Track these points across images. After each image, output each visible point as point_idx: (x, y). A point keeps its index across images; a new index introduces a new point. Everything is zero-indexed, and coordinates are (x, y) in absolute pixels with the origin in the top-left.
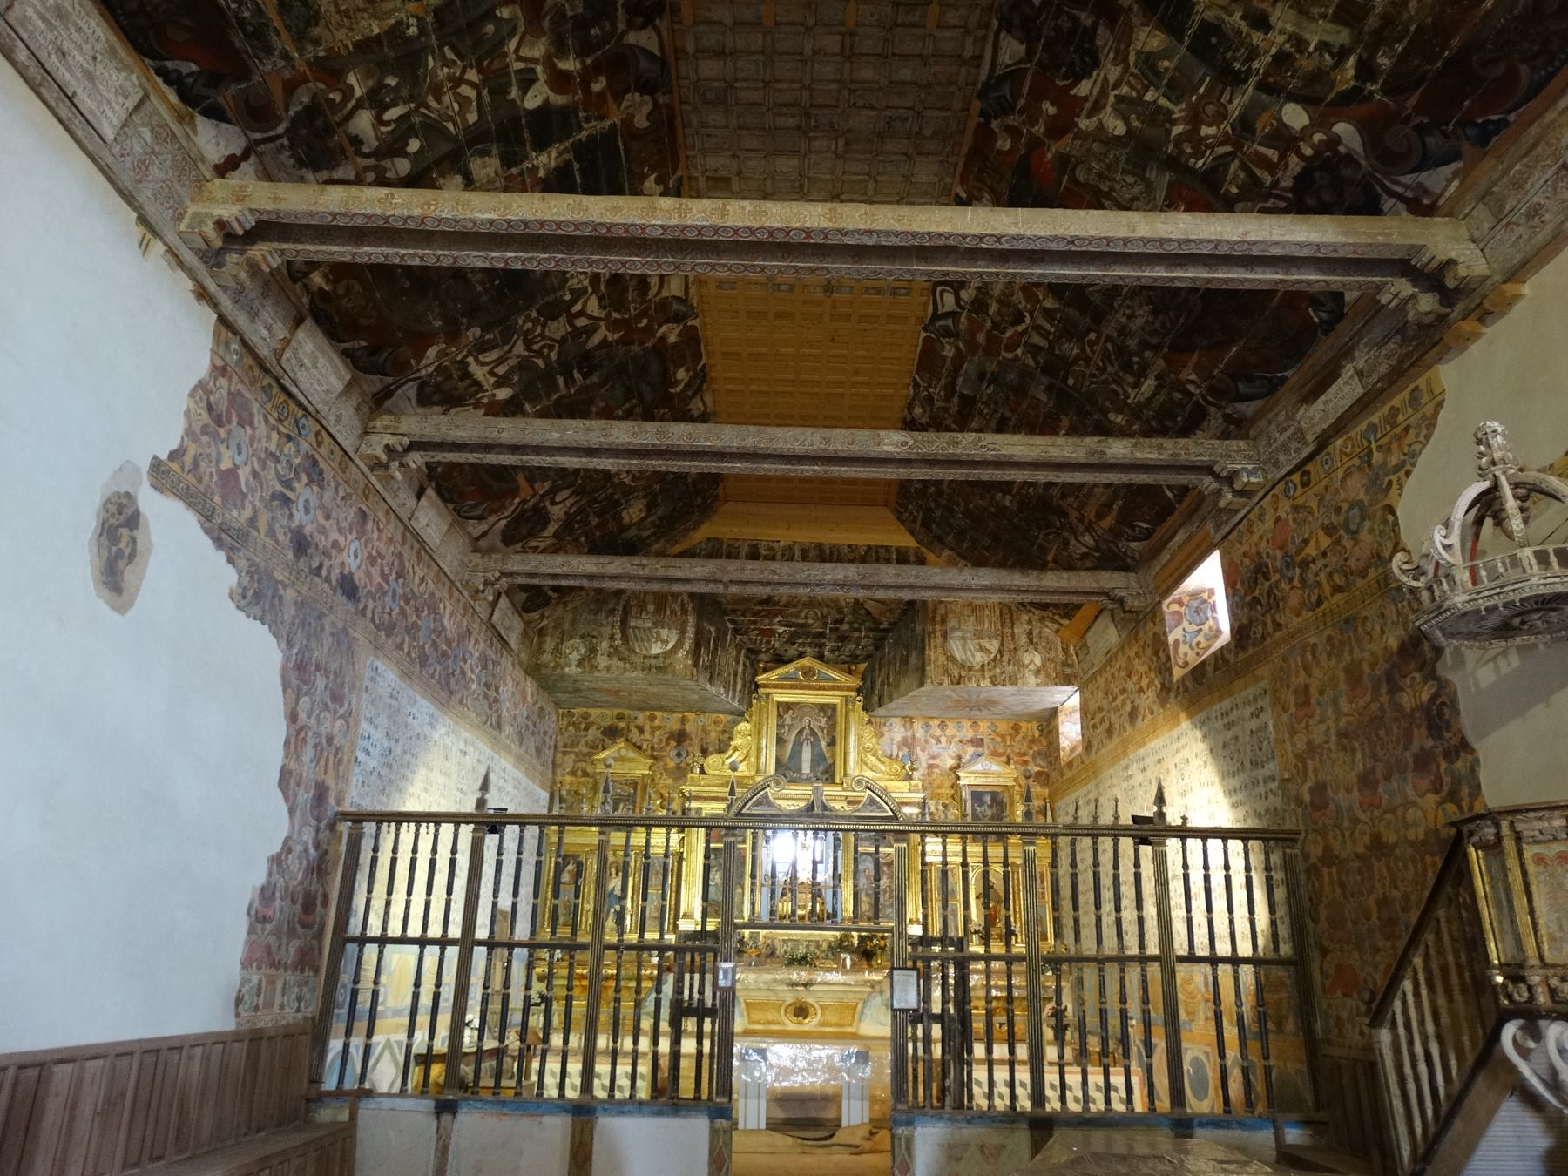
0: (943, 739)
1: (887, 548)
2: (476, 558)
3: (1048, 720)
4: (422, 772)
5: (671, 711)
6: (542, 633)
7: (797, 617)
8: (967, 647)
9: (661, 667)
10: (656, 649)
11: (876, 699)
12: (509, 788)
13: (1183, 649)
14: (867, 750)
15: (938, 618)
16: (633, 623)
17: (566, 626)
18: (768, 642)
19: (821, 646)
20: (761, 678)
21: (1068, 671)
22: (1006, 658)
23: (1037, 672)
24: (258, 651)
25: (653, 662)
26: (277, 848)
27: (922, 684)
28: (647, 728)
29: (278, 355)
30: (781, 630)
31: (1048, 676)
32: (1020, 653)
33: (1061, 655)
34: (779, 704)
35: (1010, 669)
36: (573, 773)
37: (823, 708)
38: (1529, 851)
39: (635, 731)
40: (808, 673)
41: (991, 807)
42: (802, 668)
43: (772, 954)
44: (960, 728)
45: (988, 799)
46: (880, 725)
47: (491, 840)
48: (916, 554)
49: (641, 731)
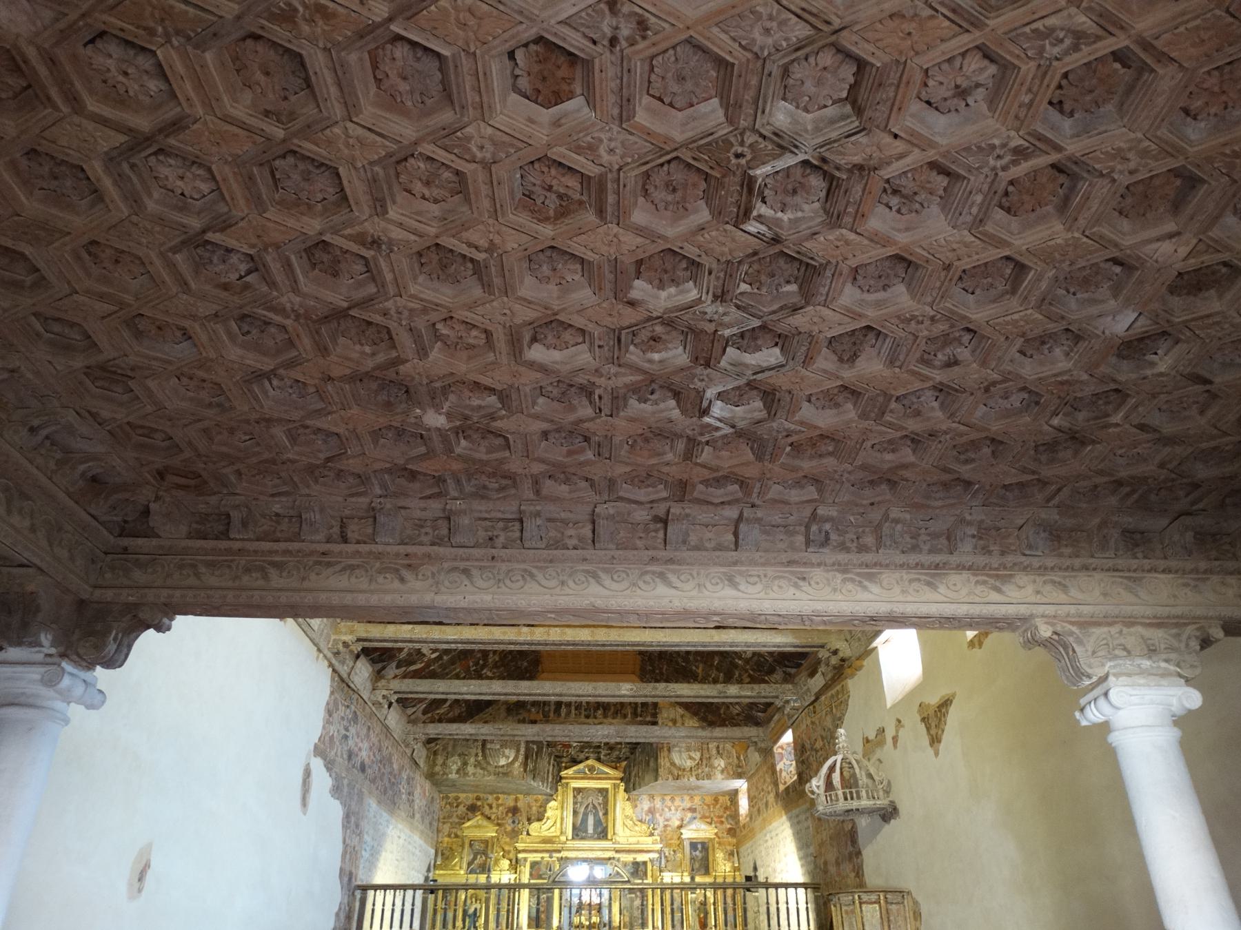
2: (410, 727)
3: (735, 793)
4: (383, 854)
5: (509, 794)
6: (435, 753)
8: (682, 758)
9: (505, 773)
10: (503, 762)
12: (417, 852)
13: (784, 774)
14: (627, 817)
17: (450, 749)
20: (563, 773)
23: (722, 772)
24: (336, 810)
26: (336, 909)
29: (349, 674)
34: (575, 789)
36: (449, 836)
38: (844, 908)
40: (592, 769)
44: (683, 800)
46: (635, 800)
47: (431, 897)
49: (491, 807)
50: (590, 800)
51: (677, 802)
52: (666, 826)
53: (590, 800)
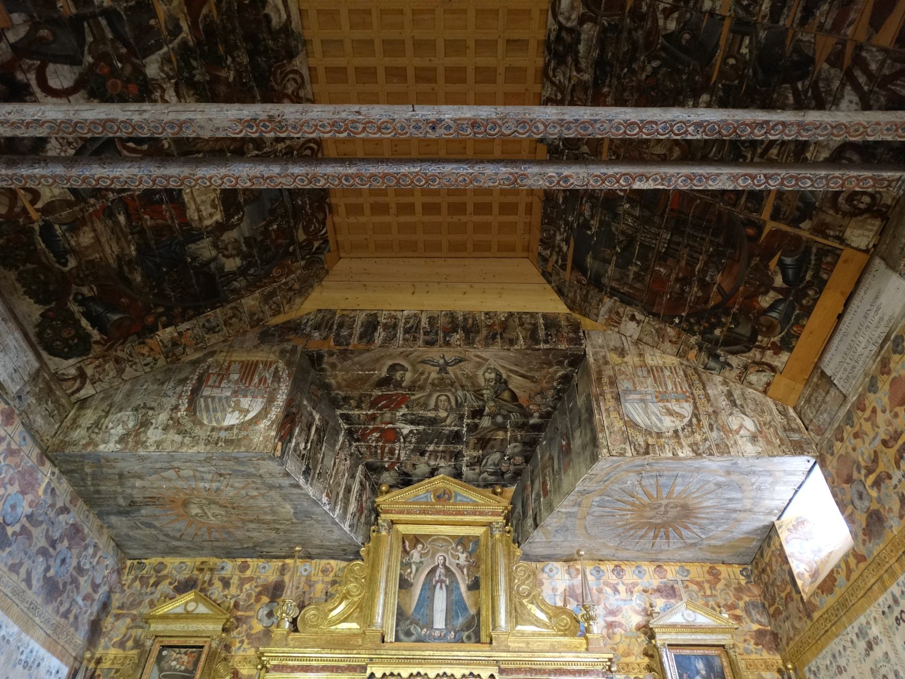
0: (621, 588)
1: (533, 315)
7: (425, 406)
10: (232, 419)
11: (530, 521)
15: (605, 380)
16: (207, 392)
17: (119, 397)
18: (392, 451)
19: (458, 456)
21: (796, 437)
22: (705, 422)
25: (223, 434)
27: (594, 458)
28: (235, 581)
30: (406, 429)
31: (769, 443)
32: (723, 416)
33: (779, 418)
34: (404, 538)
35: (714, 434)
36: (122, 645)
37: (461, 541)
39: (218, 584)
40: (442, 496)
42: (435, 491)
48: (568, 320)
49: (226, 583)
50: (439, 559)
51: (630, 575)
52: (610, 625)
53: (439, 559)
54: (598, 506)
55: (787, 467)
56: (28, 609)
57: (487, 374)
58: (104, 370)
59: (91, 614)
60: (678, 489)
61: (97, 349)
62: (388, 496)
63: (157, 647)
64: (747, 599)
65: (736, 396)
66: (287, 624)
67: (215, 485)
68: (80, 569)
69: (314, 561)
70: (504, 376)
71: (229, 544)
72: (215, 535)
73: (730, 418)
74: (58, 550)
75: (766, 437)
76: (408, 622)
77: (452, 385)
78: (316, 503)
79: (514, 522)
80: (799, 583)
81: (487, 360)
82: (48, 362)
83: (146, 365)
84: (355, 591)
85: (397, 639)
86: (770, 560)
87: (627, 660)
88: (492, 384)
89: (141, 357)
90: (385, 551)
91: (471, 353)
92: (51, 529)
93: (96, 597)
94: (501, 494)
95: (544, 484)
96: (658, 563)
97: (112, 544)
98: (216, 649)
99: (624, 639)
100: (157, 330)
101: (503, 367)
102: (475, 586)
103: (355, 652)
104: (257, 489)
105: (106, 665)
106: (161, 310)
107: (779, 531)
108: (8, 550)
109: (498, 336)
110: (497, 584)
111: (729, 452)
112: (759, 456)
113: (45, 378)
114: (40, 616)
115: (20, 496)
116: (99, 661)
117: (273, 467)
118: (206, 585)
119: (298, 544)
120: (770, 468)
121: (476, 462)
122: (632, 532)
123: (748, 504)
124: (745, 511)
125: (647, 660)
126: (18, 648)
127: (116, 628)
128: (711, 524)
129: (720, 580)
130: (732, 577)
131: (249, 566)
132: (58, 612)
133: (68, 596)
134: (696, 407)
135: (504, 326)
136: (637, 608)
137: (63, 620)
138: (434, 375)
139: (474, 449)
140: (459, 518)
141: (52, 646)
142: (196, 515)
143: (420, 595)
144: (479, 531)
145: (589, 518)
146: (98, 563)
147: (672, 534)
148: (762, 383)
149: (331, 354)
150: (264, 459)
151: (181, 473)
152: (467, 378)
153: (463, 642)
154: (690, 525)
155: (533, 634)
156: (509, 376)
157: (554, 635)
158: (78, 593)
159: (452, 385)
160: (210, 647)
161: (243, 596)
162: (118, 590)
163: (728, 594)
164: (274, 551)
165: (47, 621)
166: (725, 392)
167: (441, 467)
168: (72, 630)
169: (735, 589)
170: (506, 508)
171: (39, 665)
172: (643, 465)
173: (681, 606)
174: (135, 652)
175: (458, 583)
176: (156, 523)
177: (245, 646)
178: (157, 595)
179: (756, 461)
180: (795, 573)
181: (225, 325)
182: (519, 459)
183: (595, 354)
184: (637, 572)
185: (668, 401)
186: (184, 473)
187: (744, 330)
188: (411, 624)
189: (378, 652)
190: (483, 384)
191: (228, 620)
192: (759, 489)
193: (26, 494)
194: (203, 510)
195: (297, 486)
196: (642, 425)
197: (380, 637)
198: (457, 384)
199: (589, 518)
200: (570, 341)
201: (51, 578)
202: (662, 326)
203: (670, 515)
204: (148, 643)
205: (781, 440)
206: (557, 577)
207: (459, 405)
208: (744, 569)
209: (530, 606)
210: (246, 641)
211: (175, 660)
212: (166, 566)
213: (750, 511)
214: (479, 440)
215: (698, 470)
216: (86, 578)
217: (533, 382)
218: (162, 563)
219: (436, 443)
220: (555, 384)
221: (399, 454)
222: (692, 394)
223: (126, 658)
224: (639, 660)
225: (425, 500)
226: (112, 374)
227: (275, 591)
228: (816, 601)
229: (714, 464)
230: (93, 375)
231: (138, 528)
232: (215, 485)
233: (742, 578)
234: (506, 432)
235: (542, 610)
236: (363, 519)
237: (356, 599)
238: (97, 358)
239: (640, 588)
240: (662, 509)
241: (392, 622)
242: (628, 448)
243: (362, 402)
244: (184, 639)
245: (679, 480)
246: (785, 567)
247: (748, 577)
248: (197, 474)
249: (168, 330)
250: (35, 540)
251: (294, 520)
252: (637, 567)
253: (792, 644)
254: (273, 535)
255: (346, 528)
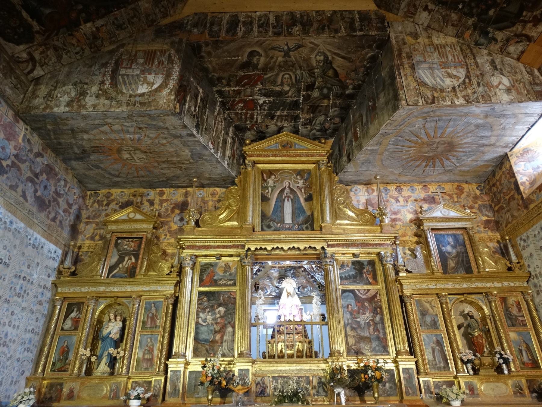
0: (401, 199)
1: (351, 12)
7: (274, 83)
10: (143, 89)
11: (345, 158)
15: (404, 55)
16: (123, 71)
17: (61, 77)
18: (252, 117)
19: (296, 118)
22: (474, 81)
25: (138, 99)
27: (396, 108)
28: (157, 201)
30: (262, 100)
31: (519, 93)
32: (487, 77)
33: (527, 77)
34: (263, 172)
35: (481, 89)
36: (92, 238)
37: (300, 173)
39: (146, 204)
40: (286, 146)
41: (454, 247)
42: (281, 142)
43: (262, 393)
45: (451, 240)
48: (376, 14)
49: (152, 203)
50: (286, 184)
51: (406, 191)
52: (394, 220)
53: (286, 184)
54: (393, 145)
55: (528, 111)
56: (28, 214)
57: (318, 57)
58: (47, 56)
59: (70, 221)
60: (449, 130)
61: (39, 38)
62: (251, 146)
63: (114, 239)
64: (480, 203)
65: (497, 63)
66: (193, 223)
67: (137, 136)
68: (57, 193)
69: (205, 189)
70: (330, 58)
71: (151, 179)
72: (142, 173)
73: (492, 78)
74: (41, 179)
75: (517, 89)
76: (269, 220)
77: (293, 66)
78: (205, 147)
79: (333, 162)
80: (522, 188)
81: (318, 46)
82: (5, 47)
83: (77, 53)
84: (233, 204)
85: (262, 230)
86: (501, 177)
87: (404, 239)
88: (321, 64)
89: (72, 47)
90: (251, 180)
91: (307, 40)
92: (33, 166)
93: (72, 211)
94: (324, 143)
95: (355, 133)
96: (424, 184)
97: (76, 180)
98: (151, 238)
99: (402, 227)
100: (80, 25)
101: (329, 51)
102: (309, 199)
103: (237, 237)
104: (165, 138)
105: (85, 249)
106: (80, 7)
107: (510, 158)
108: (6, 176)
109: (326, 28)
110: (324, 197)
111: (491, 100)
112: (511, 102)
113: (5, 58)
114: (37, 219)
115: (7, 142)
116: (80, 248)
117: (174, 121)
118: (139, 204)
119: (194, 177)
120: (516, 111)
121: (309, 122)
122: (411, 163)
123: (493, 140)
124: (490, 145)
125: (416, 239)
126: (27, 236)
127: (87, 230)
128: (464, 156)
129: (463, 193)
130: (471, 190)
131: (164, 193)
132: (48, 218)
133: (53, 209)
134: (468, 71)
135: (331, 20)
136: (411, 210)
137: (52, 223)
138: (280, 59)
139: (308, 113)
140: (298, 158)
141: (49, 238)
142: (127, 159)
143: (275, 205)
144: (311, 167)
145: (386, 153)
146: (68, 191)
147: (438, 164)
148: (518, 52)
149: (207, 44)
150: (168, 115)
151: (113, 127)
152: (304, 60)
153: (303, 230)
154: (450, 157)
155: (347, 225)
156: (333, 58)
157: (360, 225)
158: (59, 208)
159: (293, 66)
160: (147, 237)
161: (163, 210)
162: (84, 208)
163: (468, 200)
164: (180, 183)
165: (42, 222)
166: (490, 60)
167: (285, 127)
168: (60, 229)
169: (473, 197)
170: (328, 152)
171: (42, 247)
172: (429, 112)
173: (441, 207)
174: (100, 242)
175: (298, 197)
176: (102, 166)
177: (168, 237)
178: (109, 210)
179: (509, 106)
180: (519, 182)
181: (129, 24)
182: (337, 120)
183: (396, 37)
184: (411, 190)
185: (448, 68)
186: (116, 127)
187: (513, 8)
188: (270, 221)
189: (251, 237)
190: (315, 65)
191: (156, 222)
192: (504, 128)
193: (11, 141)
194: (131, 155)
195: (192, 135)
196: (430, 84)
197: (252, 229)
198: (297, 65)
199: (386, 153)
200: (378, 29)
201: (39, 197)
202: (448, 13)
203: (439, 150)
204: (108, 236)
205: (527, 91)
206: (359, 194)
207: (298, 81)
208: (479, 186)
209: (345, 209)
210: (168, 235)
211: (126, 245)
212: (112, 194)
213: (493, 145)
214: (311, 106)
215: (466, 115)
216: (62, 199)
217: (350, 62)
218: (110, 193)
219: (282, 110)
220: (365, 63)
221: (257, 118)
222: (466, 62)
223: (96, 245)
224: (411, 239)
225: (275, 148)
226: (54, 59)
227: (183, 207)
228: (534, 197)
229: (477, 110)
230: (40, 60)
231: (90, 169)
232: (137, 136)
233: (477, 191)
234: (329, 100)
235: (352, 212)
236: (235, 161)
237: (234, 208)
238: (41, 46)
239: (413, 198)
240: (435, 145)
241: (258, 221)
242: (420, 100)
243: (230, 81)
244: (129, 234)
245: (451, 123)
246: (512, 180)
247: (481, 190)
248: (124, 128)
249: (89, 25)
250: (23, 172)
251: (191, 161)
252: (411, 187)
253: (509, 226)
254: (178, 171)
255: (226, 166)
